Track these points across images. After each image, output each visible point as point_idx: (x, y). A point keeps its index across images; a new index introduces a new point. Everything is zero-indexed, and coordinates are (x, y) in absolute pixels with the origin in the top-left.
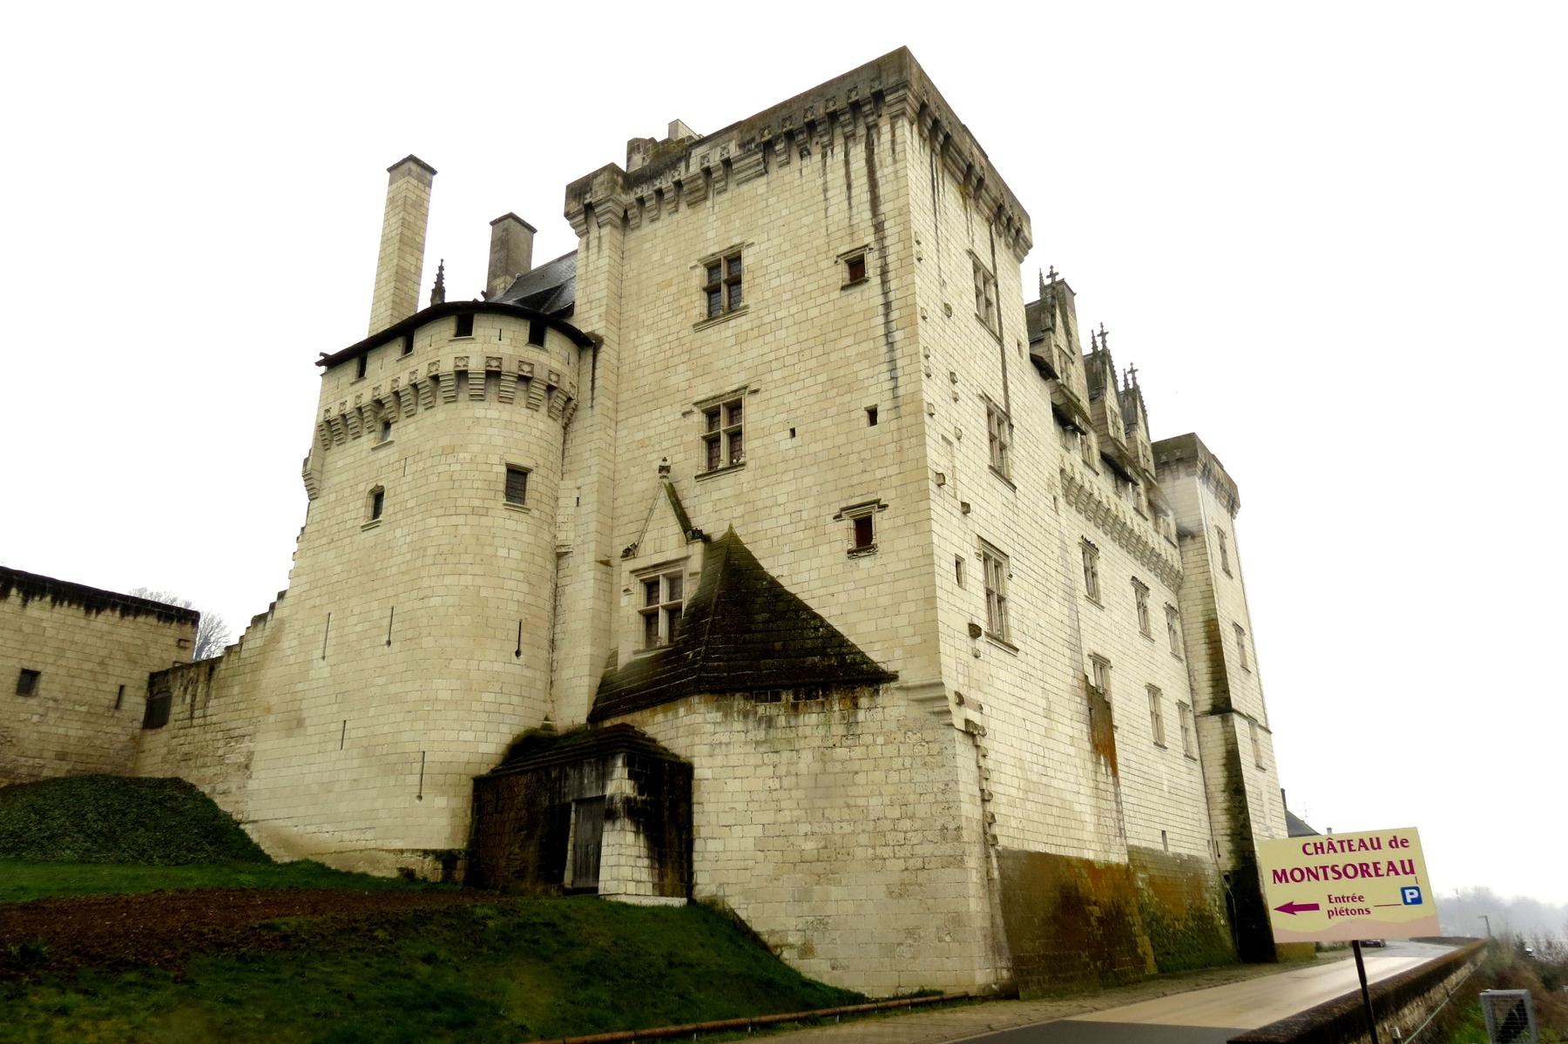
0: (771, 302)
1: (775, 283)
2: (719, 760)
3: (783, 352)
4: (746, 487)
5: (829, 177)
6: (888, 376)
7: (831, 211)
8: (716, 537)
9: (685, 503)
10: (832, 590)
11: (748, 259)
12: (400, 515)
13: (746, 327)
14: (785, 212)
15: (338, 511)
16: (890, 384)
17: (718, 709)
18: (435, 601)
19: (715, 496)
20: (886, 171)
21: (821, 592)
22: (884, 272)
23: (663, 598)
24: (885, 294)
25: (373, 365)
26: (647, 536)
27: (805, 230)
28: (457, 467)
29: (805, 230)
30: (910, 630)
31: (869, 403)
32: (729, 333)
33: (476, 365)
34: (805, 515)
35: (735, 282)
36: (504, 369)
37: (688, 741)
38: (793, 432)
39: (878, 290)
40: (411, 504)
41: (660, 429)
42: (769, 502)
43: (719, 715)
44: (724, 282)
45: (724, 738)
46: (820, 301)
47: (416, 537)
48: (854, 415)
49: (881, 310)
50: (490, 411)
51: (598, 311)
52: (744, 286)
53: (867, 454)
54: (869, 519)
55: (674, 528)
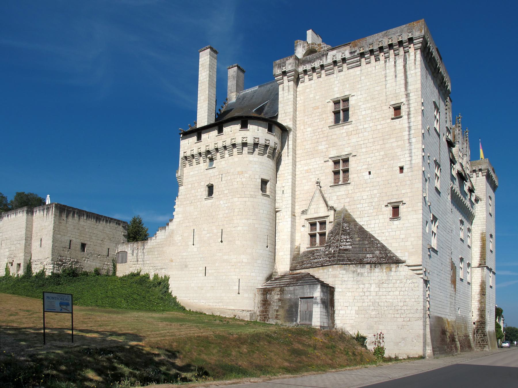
0: (362, 120)
1: (363, 113)
2: (344, 286)
3: (367, 141)
4: (350, 192)
5: (388, 71)
6: (408, 155)
7: (388, 86)
8: (338, 209)
9: (325, 196)
10: (382, 231)
11: (352, 101)
12: (221, 196)
13: (351, 129)
14: (368, 84)
15: (193, 191)
16: (409, 159)
17: (344, 269)
18: (239, 228)
19: (338, 194)
20: (412, 72)
21: (379, 231)
22: (409, 114)
23: (318, 230)
25: (204, 136)
26: (312, 207)
27: (376, 92)
28: (244, 179)
29: (376, 92)
30: (411, 247)
31: (401, 165)
32: (344, 131)
33: (250, 141)
34: (374, 204)
35: (346, 111)
36: (260, 142)
37: (333, 279)
38: (370, 173)
39: (406, 121)
40: (226, 192)
41: (315, 166)
42: (360, 198)
43: (345, 271)
44: (341, 112)
45: (346, 279)
46: (382, 122)
47: (229, 204)
48: (394, 169)
49: (407, 129)
50: (256, 158)
51: (289, 117)
52: (350, 113)
53: (399, 184)
54: (398, 207)
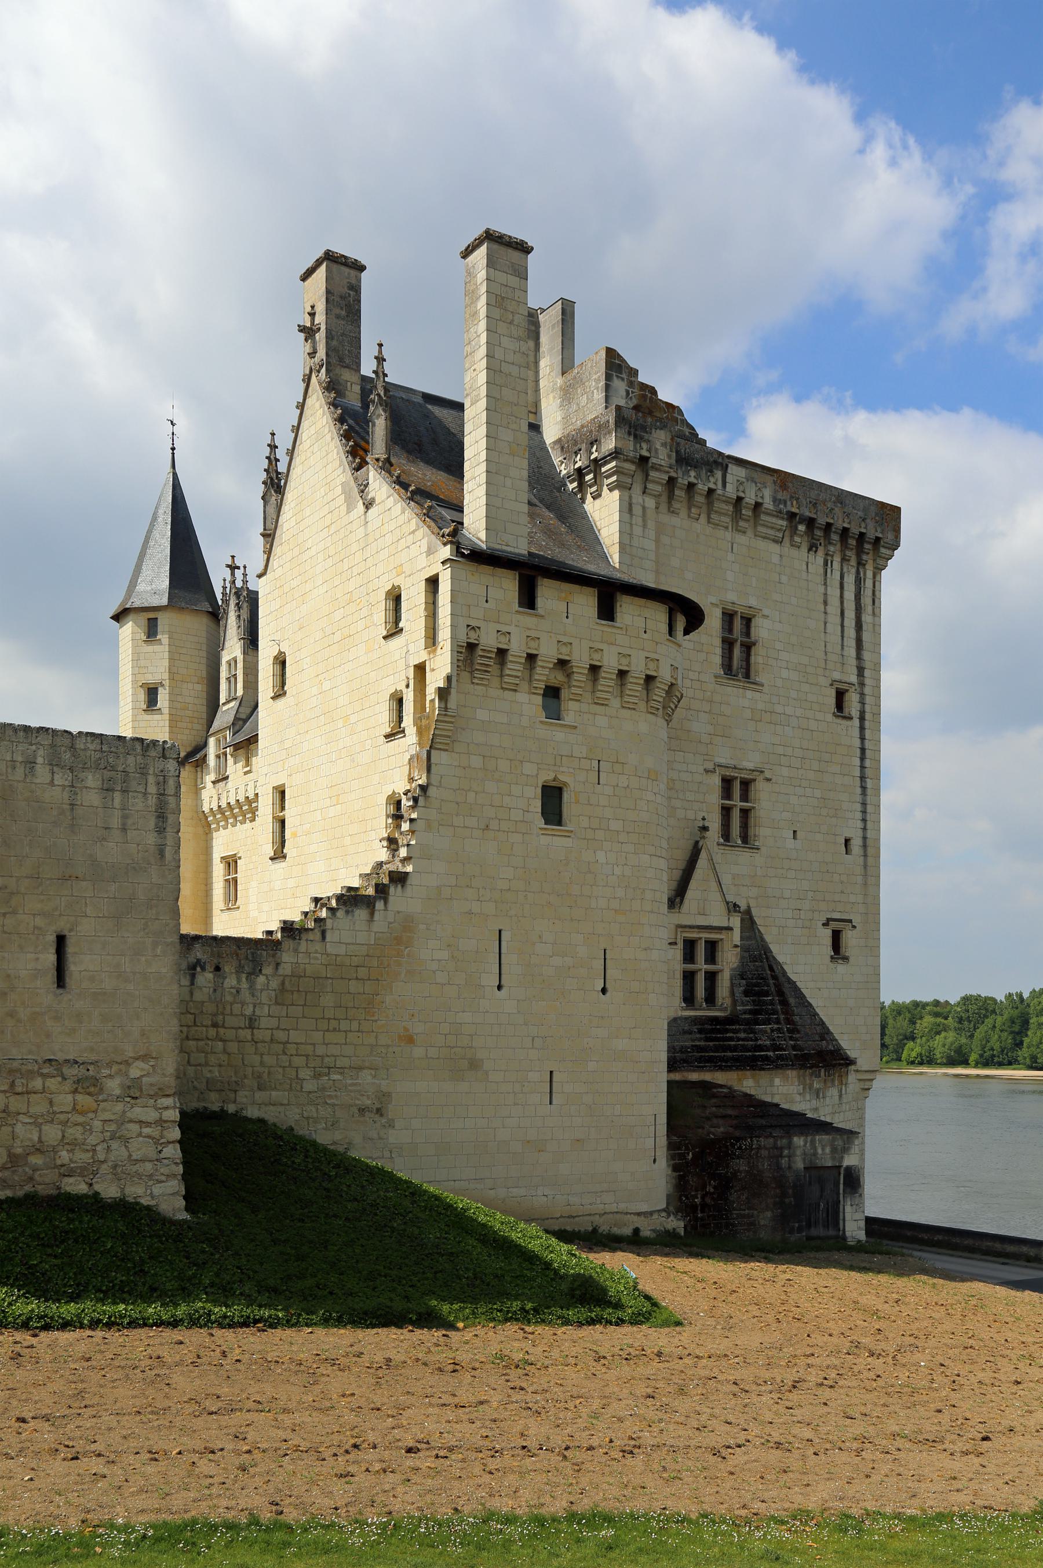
1: (785, 674)
12: (600, 835)
13: (761, 706)
22: (862, 719)
24: (862, 738)
31: (848, 835)
40: (615, 825)
55: (718, 896)
